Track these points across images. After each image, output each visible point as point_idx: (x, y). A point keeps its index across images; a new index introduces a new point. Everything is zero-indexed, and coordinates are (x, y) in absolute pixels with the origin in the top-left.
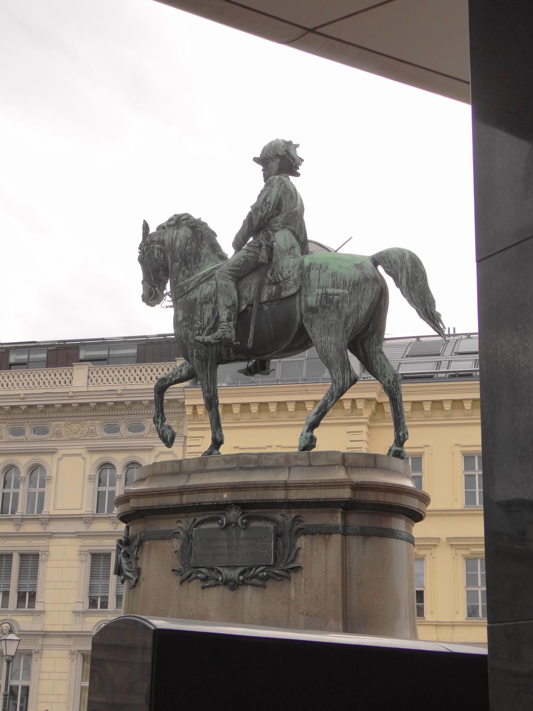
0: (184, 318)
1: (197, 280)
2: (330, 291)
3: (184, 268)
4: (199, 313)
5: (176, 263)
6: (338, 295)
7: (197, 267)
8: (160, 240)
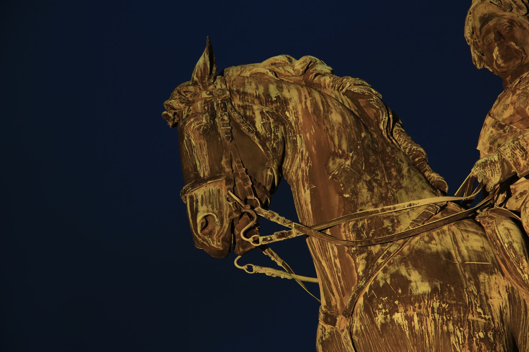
0: (434, 290)
1: (414, 215)
3: (369, 178)
4: (473, 288)
5: (338, 160)
7: (399, 186)
8: (267, 95)
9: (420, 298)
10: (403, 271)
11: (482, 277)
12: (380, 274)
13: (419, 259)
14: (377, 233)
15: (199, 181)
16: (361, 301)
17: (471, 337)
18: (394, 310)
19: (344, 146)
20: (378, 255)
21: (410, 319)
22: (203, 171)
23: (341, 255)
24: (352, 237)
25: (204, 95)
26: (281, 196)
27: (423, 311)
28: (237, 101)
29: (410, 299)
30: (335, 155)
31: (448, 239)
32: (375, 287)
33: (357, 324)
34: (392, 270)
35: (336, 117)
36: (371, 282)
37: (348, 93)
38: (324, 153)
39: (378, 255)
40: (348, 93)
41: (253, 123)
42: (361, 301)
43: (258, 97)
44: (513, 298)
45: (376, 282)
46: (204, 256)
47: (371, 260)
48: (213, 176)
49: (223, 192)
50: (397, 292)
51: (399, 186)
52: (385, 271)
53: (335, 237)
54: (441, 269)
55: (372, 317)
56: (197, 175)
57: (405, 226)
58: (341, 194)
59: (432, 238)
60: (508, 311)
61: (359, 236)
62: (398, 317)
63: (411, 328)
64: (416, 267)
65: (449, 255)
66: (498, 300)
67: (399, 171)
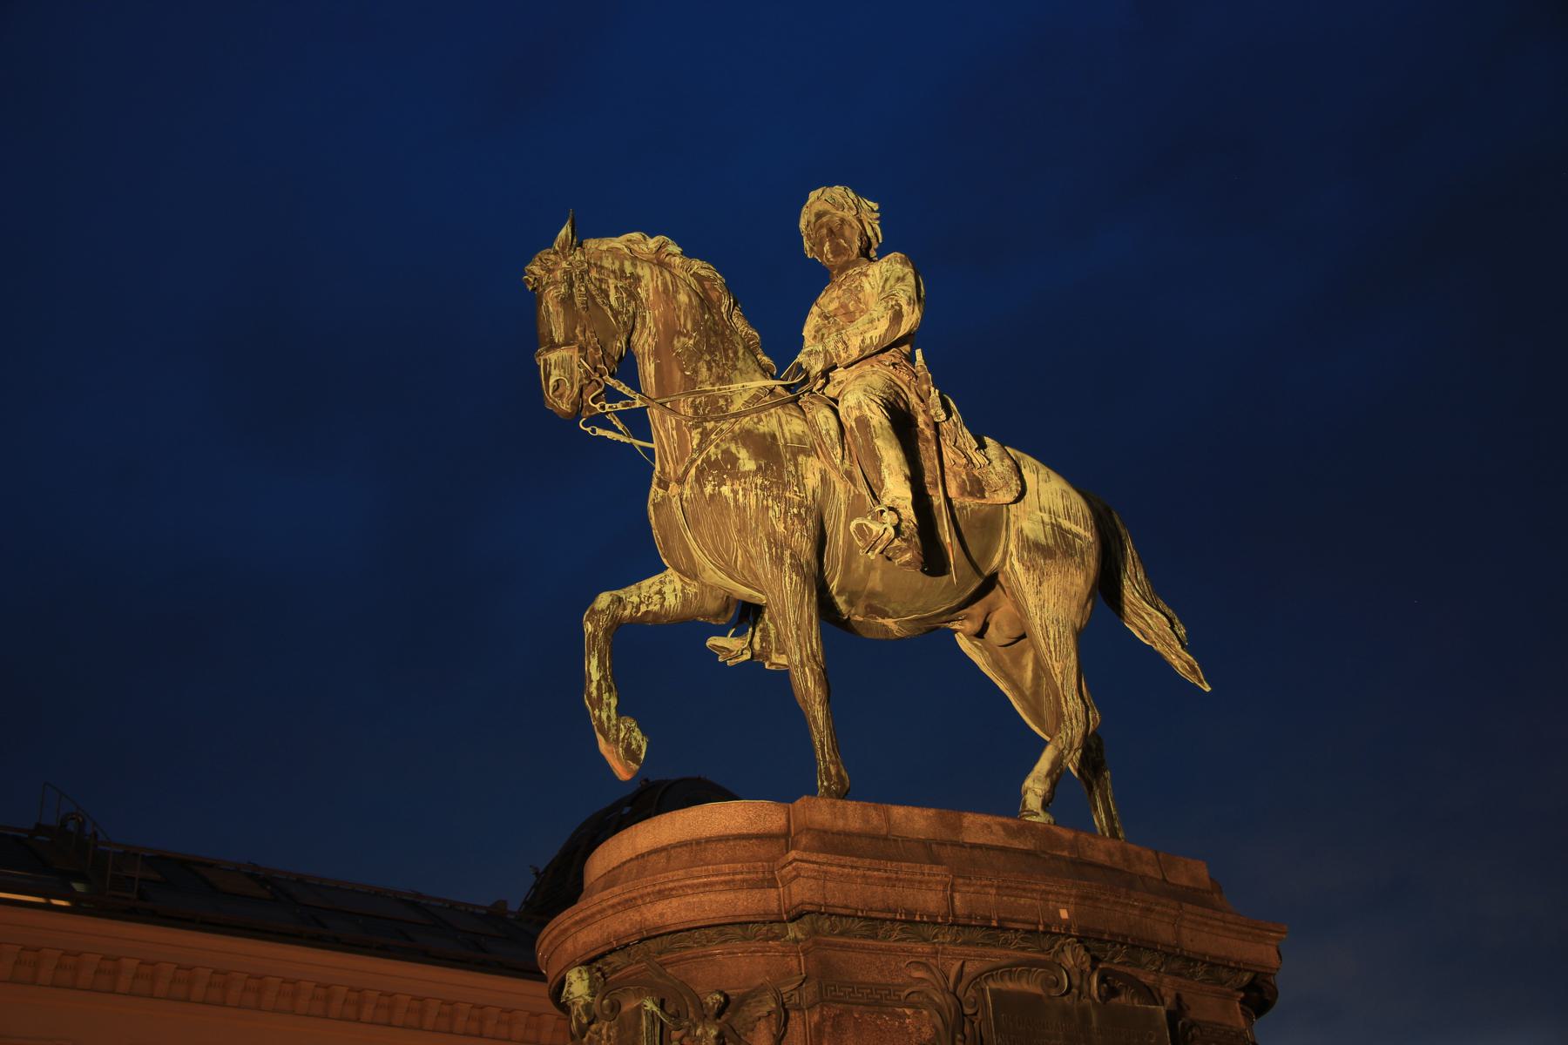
0: (759, 468)
1: (746, 397)
2: (1066, 524)
3: (708, 358)
4: (792, 468)
6: (1077, 535)
7: (734, 367)
8: (622, 271)
9: (746, 475)
10: (733, 449)
11: (801, 459)
12: (712, 449)
13: (746, 437)
14: (714, 410)
15: (554, 346)
16: (693, 471)
17: (786, 512)
18: (720, 485)
19: (689, 326)
20: (712, 431)
21: (735, 492)
22: (558, 336)
23: (678, 427)
24: (690, 412)
25: (564, 264)
26: (627, 367)
27: (748, 486)
28: (594, 274)
29: (736, 475)
30: (680, 333)
31: (774, 421)
32: (707, 460)
33: (687, 492)
34: (724, 446)
35: (683, 298)
36: (704, 455)
37: (695, 275)
38: (670, 332)
39: (712, 431)
40: (695, 275)
41: (608, 296)
42: (693, 471)
43: (614, 272)
44: (824, 480)
45: (709, 457)
46: (552, 415)
47: (705, 435)
48: (567, 343)
49: (576, 359)
50: (725, 467)
51: (734, 367)
52: (717, 446)
53: (674, 411)
54: (766, 449)
55: (702, 487)
56: (552, 340)
57: (737, 406)
58: (683, 371)
59: (760, 420)
60: (819, 491)
61: (696, 412)
62: (726, 490)
63: (736, 501)
64: (745, 445)
65: (774, 436)
66: (812, 481)
67: (736, 353)
